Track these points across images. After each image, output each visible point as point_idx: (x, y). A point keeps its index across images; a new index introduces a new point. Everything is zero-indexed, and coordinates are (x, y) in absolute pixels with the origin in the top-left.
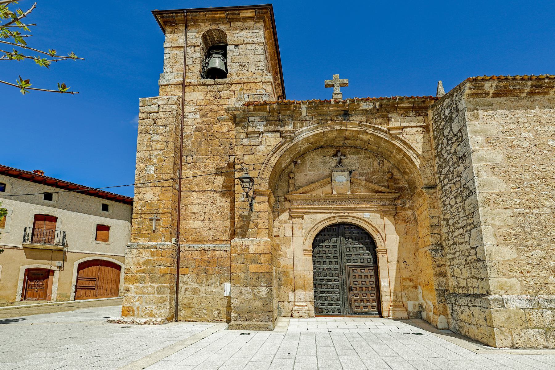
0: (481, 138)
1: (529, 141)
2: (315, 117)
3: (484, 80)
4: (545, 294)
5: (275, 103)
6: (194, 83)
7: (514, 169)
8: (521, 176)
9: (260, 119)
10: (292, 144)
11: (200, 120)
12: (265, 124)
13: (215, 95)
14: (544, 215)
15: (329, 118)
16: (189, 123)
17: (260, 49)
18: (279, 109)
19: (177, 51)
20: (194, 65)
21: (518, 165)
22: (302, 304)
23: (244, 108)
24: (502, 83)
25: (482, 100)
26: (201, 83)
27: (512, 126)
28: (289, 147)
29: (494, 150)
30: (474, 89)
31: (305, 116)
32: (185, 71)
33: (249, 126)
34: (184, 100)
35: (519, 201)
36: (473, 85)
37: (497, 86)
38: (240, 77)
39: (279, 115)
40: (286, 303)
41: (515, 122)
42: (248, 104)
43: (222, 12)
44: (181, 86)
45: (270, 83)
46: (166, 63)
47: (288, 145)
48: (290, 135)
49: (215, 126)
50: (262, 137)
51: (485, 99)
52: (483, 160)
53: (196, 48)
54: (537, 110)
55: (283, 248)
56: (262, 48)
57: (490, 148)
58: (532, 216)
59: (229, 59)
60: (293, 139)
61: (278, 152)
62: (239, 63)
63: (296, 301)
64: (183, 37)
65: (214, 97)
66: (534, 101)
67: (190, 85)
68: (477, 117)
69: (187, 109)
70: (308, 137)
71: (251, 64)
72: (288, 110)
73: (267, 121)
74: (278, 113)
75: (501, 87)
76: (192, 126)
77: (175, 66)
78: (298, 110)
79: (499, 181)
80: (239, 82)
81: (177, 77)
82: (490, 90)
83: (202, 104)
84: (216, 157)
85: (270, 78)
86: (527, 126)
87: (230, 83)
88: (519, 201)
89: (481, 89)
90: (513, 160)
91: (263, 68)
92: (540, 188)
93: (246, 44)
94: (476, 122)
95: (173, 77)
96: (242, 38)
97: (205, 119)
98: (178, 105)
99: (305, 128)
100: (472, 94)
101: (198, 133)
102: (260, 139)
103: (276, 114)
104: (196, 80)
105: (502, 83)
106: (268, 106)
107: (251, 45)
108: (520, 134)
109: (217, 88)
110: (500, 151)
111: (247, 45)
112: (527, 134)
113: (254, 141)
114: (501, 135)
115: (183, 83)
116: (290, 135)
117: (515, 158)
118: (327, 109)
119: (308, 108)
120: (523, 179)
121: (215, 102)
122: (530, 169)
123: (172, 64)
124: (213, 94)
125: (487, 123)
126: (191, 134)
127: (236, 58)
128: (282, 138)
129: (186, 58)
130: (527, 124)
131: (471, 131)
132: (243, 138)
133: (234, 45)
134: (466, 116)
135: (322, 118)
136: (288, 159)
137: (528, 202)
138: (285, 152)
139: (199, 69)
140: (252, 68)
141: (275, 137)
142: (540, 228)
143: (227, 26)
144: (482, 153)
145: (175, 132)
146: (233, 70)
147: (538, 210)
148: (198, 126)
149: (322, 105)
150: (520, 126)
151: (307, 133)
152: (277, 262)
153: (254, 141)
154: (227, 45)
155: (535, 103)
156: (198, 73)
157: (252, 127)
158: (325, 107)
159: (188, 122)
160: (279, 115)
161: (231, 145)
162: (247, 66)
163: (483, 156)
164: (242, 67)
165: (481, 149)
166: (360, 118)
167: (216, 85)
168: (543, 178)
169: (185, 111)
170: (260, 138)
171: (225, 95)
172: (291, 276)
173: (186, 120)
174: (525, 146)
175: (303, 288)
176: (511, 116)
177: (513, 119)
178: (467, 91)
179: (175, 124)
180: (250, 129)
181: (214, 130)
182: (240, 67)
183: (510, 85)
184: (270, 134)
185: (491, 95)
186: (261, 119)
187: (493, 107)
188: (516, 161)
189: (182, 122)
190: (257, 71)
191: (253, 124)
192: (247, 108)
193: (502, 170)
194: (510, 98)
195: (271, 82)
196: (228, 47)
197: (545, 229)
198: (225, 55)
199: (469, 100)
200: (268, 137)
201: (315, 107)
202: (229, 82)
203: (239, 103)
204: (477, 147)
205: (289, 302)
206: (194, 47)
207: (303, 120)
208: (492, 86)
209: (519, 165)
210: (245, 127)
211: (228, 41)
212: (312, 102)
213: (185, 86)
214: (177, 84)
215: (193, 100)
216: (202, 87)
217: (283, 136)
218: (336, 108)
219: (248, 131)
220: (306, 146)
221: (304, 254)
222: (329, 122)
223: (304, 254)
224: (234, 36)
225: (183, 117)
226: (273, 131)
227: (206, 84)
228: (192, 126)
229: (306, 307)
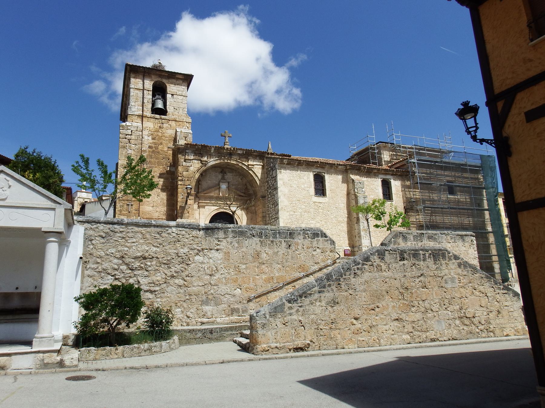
15: (223, 155)
31: (212, 153)
64: (142, 83)
153: (188, 164)
155: (299, 169)
161: (169, 160)
206: (148, 91)
222: (223, 158)
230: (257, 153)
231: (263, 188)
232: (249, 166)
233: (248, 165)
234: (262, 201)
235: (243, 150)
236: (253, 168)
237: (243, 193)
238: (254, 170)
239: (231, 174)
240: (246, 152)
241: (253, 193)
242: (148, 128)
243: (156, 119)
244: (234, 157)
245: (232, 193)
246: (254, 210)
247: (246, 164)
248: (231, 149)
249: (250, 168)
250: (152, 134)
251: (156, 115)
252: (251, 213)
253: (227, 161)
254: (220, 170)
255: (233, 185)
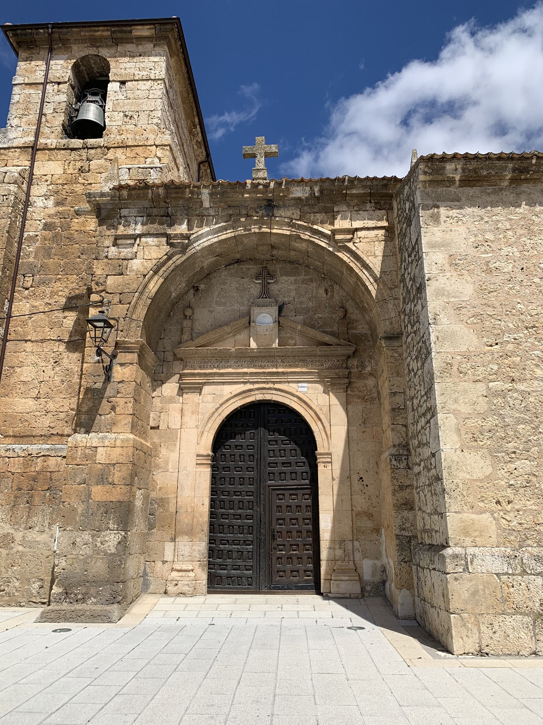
0: (441, 256)
1: (512, 261)
2: (223, 209)
3: (445, 159)
4: (535, 545)
5: (162, 186)
6: (52, 145)
7: (490, 311)
8: (500, 322)
9: (138, 213)
10: (185, 257)
11: (52, 211)
12: (145, 220)
13: (82, 167)
14: (534, 394)
15: (244, 212)
16: (35, 216)
17: (159, 90)
18: (167, 196)
19: (32, 91)
20: (55, 114)
21: (495, 302)
22: (184, 567)
23: (113, 193)
24: (471, 164)
25: (446, 191)
26: (62, 145)
27: (489, 236)
28: (179, 262)
29: (460, 277)
30: (430, 174)
31: (208, 209)
32: (40, 123)
33: (120, 224)
34: (32, 174)
35: (495, 367)
36: (429, 168)
37: (463, 170)
38: (123, 137)
39: (167, 205)
40: (159, 564)
41: (493, 229)
42: (120, 188)
43: (106, 28)
44: (30, 150)
45: (168, 148)
46: (14, 111)
47: (178, 259)
48: (182, 241)
49: (76, 220)
50: (138, 245)
51: (450, 189)
52: (444, 295)
53: (61, 86)
54: (524, 209)
55: (163, 451)
56: (161, 87)
57: (455, 274)
58: (515, 395)
59: (109, 105)
60: (186, 249)
61: (161, 272)
62: (123, 112)
63: (176, 560)
64: (44, 67)
65: (80, 170)
66: (520, 193)
67: (44, 149)
68: (436, 219)
69: (35, 190)
70: (211, 245)
71: (142, 114)
72: (182, 198)
73: (149, 216)
74: (165, 202)
75: (469, 171)
76: (40, 221)
77: (26, 115)
78: (197, 198)
79: (466, 332)
80: (121, 145)
81: (26, 134)
82: (454, 176)
83: (60, 182)
84: (71, 276)
85: (167, 138)
86: (511, 236)
87: (106, 147)
88: (495, 367)
89: (441, 174)
90: (489, 295)
91: (159, 122)
92: (529, 345)
93: (138, 80)
94: (435, 229)
95: (19, 134)
96: (133, 71)
97: (61, 209)
98: (20, 184)
99: (206, 229)
100: (430, 181)
101: (47, 232)
102: (135, 249)
103: (162, 204)
104: (56, 141)
105: (471, 164)
106: (150, 191)
107: (145, 82)
108: (500, 250)
109: (85, 154)
110: (469, 279)
111: (139, 82)
112: (509, 249)
113: (126, 252)
114: (472, 251)
115: (34, 144)
116: (182, 241)
117: (492, 292)
118: (240, 197)
119: (211, 195)
120: (504, 328)
121: (80, 178)
122: (514, 311)
123: (21, 112)
124: (79, 164)
125: (451, 230)
126: (37, 236)
127: (121, 104)
128: (169, 247)
129: (44, 102)
130: (510, 233)
131: (428, 243)
132: (108, 245)
133: (119, 81)
134: (421, 218)
135: (233, 211)
136: (180, 284)
137: (510, 369)
138: (172, 271)
139: (62, 122)
140: (143, 121)
141: (157, 245)
142: (528, 418)
143: (112, 51)
144: (443, 282)
145: (8, 232)
146: (114, 123)
147: (525, 384)
148: (49, 220)
149: (233, 190)
150: (501, 236)
151: (210, 237)
152: (150, 479)
154: (109, 81)
156: (60, 129)
157: (124, 226)
158: (237, 192)
159: (34, 214)
160: (167, 205)
162: (135, 117)
163: (444, 288)
164: (127, 120)
165: (441, 274)
166: (291, 212)
167: (84, 149)
168: (533, 327)
169: (31, 194)
170: (136, 245)
171: (96, 167)
172: (172, 509)
173: (31, 209)
174: (506, 270)
175: (190, 532)
176: (486, 219)
177: (490, 223)
178: (422, 177)
179: (10, 218)
180: (121, 230)
181: (73, 228)
182: (125, 120)
183: (482, 168)
184: (151, 239)
185: (457, 183)
186: (139, 212)
187: (461, 203)
188: (494, 296)
189: (25, 213)
190: (149, 127)
191: (126, 221)
192: (118, 193)
193: (472, 311)
194: (486, 189)
195: (169, 145)
196: (110, 85)
197: (535, 419)
198: (104, 98)
199: (427, 190)
200: (147, 245)
201: (223, 194)
202: (105, 145)
203: (108, 184)
204: (435, 271)
205: (164, 562)
206: (59, 83)
207: (205, 216)
208: (456, 169)
209: (497, 304)
210: (114, 226)
211: (110, 75)
212: (218, 185)
213: (37, 150)
214: (24, 147)
215: (46, 175)
216: (63, 152)
217: (171, 243)
218: (254, 195)
219: (117, 234)
220: (211, 260)
221: (197, 464)
222: (243, 219)
223: (197, 464)
224: (121, 67)
225: (27, 203)
226: (157, 234)
227: (70, 147)
228: (40, 221)
229: (191, 574)
230: (365, 187)
231: (391, 306)
232: (338, 237)
233: (334, 232)
234: (390, 353)
235: (310, 183)
236: (350, 240)
237: (333, 334)
238: (354, 248)
239: (292, 278)
240: (321, 191)
241: (369, 332)
242: (49, 177)
243: (73, 149)
244: (282, 214)
245: (292, 338)
246: (374, 390)
247: (326, 230)
248: (266, 186)
249: (341, 241)
250: (57, 192)
251: (73, 140)
252: (363, 399)
253: (260, 228)
254: (254, 269)
255: (297, 312)
